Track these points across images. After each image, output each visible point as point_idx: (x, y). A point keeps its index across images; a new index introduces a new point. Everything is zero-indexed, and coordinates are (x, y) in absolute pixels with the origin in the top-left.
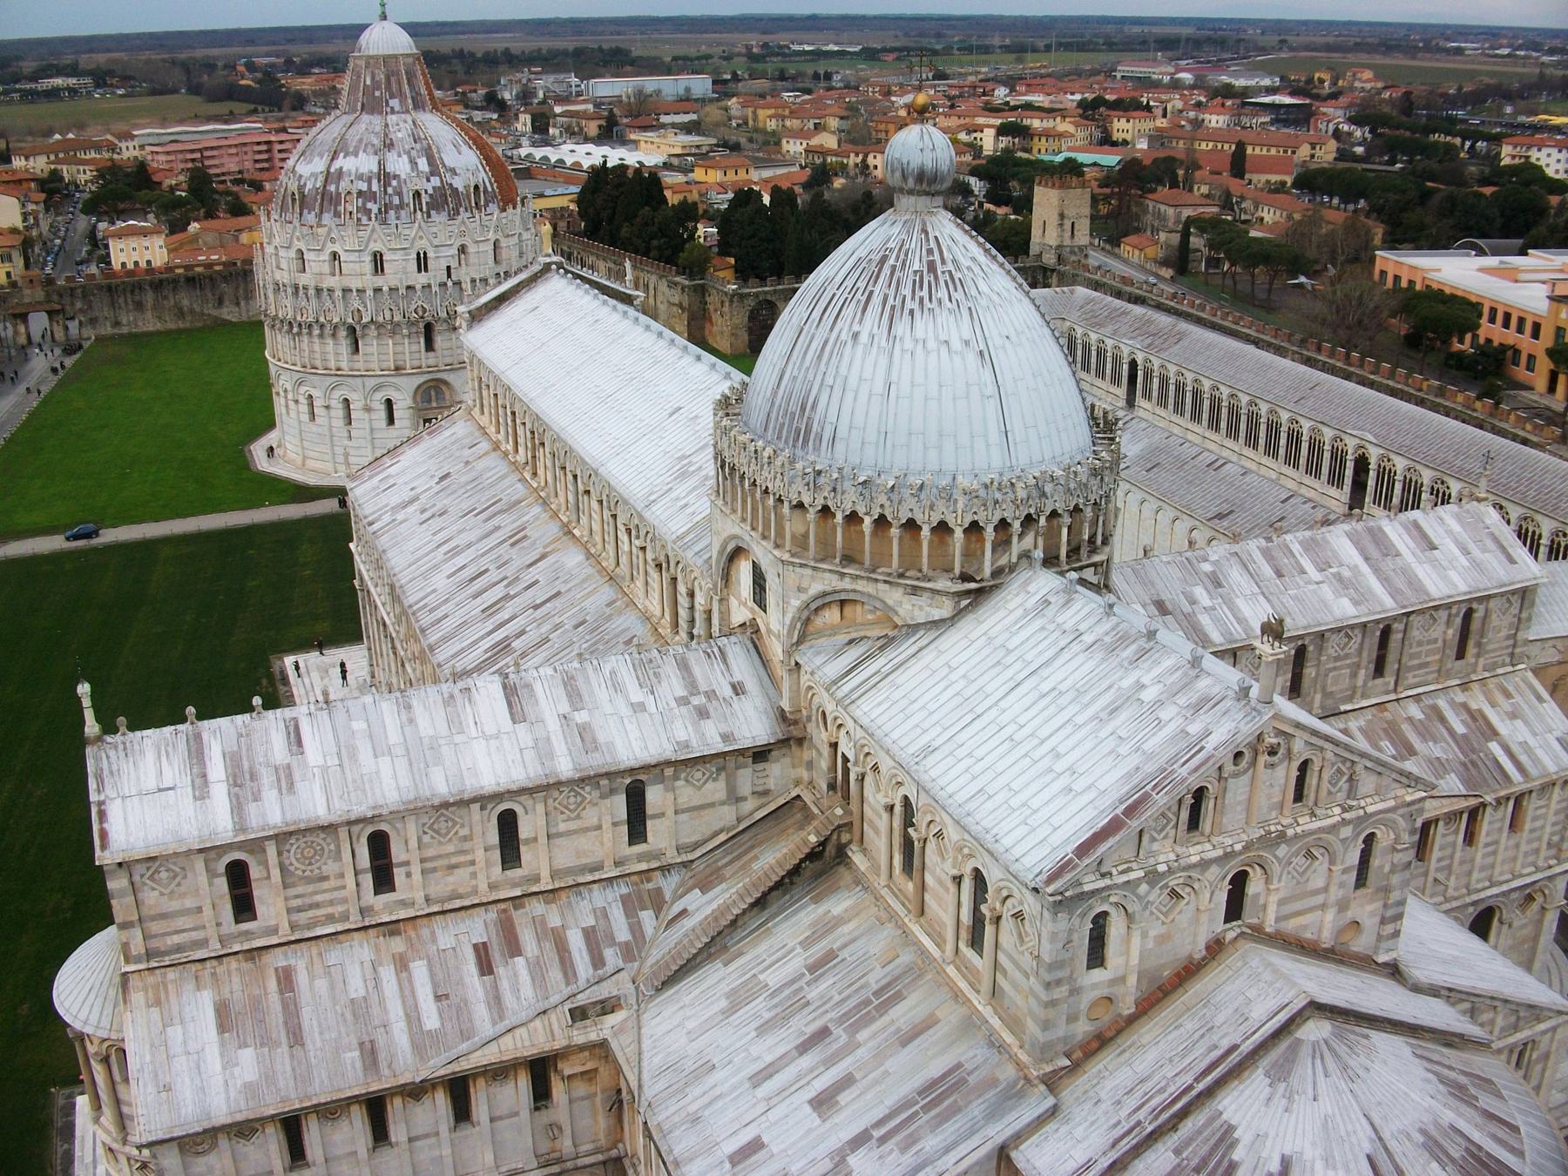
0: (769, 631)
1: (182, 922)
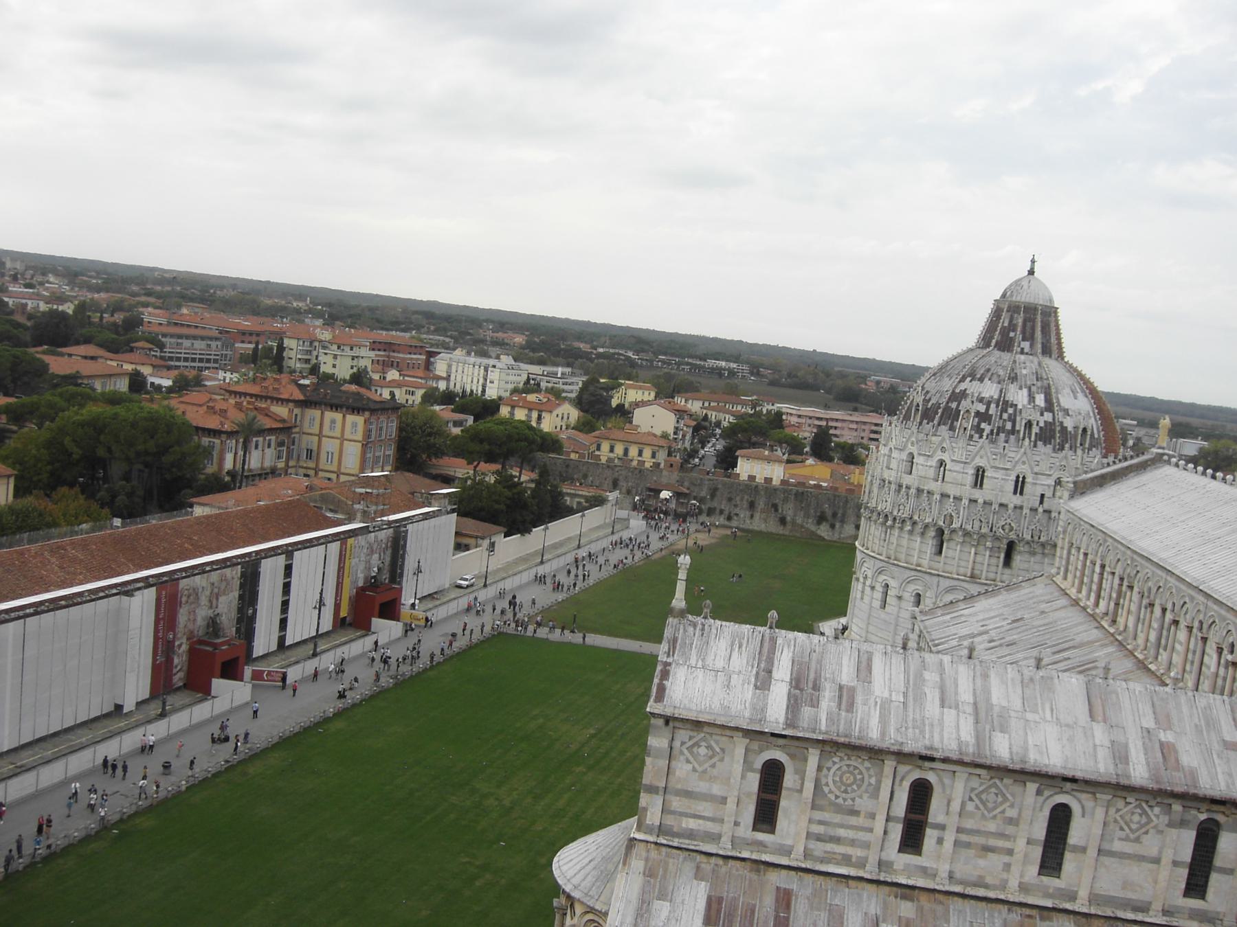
1: (705, 808)
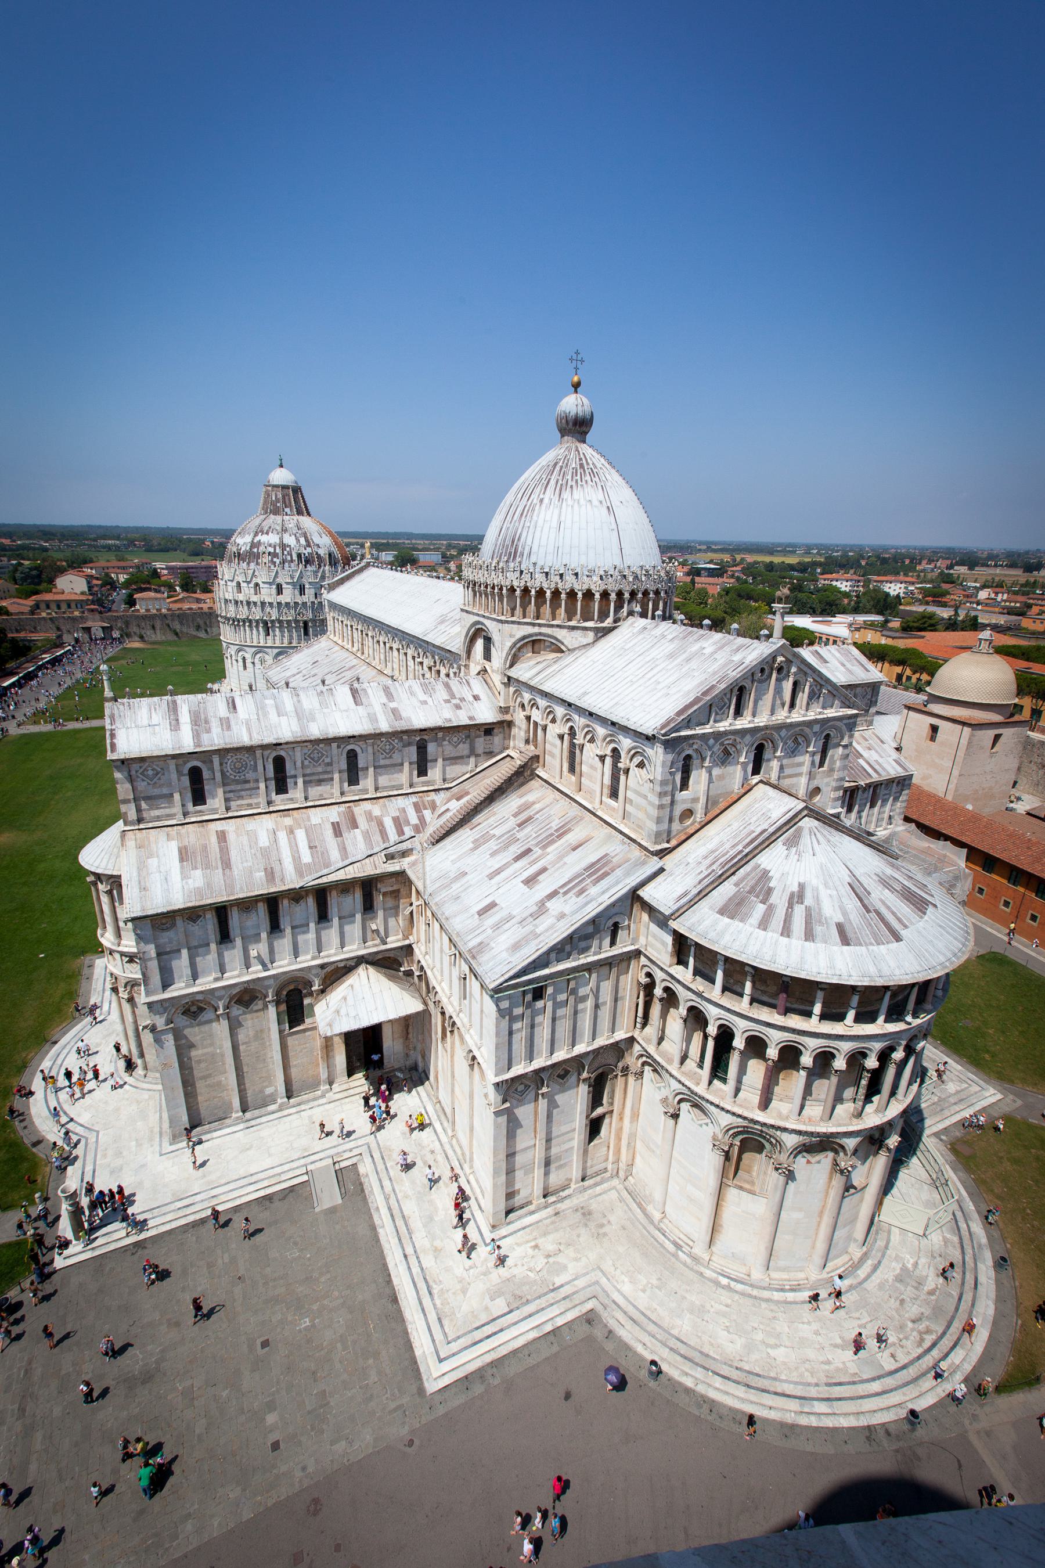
0: (493, 671)
